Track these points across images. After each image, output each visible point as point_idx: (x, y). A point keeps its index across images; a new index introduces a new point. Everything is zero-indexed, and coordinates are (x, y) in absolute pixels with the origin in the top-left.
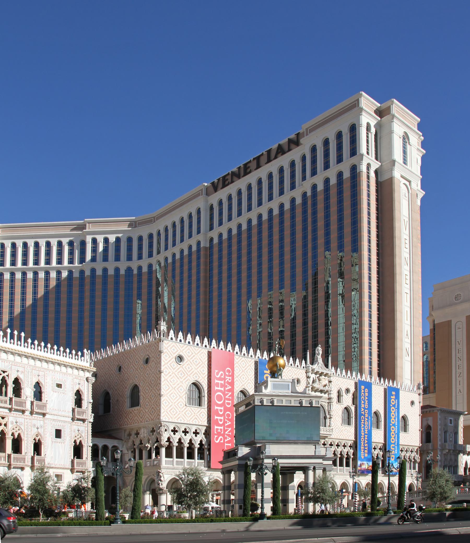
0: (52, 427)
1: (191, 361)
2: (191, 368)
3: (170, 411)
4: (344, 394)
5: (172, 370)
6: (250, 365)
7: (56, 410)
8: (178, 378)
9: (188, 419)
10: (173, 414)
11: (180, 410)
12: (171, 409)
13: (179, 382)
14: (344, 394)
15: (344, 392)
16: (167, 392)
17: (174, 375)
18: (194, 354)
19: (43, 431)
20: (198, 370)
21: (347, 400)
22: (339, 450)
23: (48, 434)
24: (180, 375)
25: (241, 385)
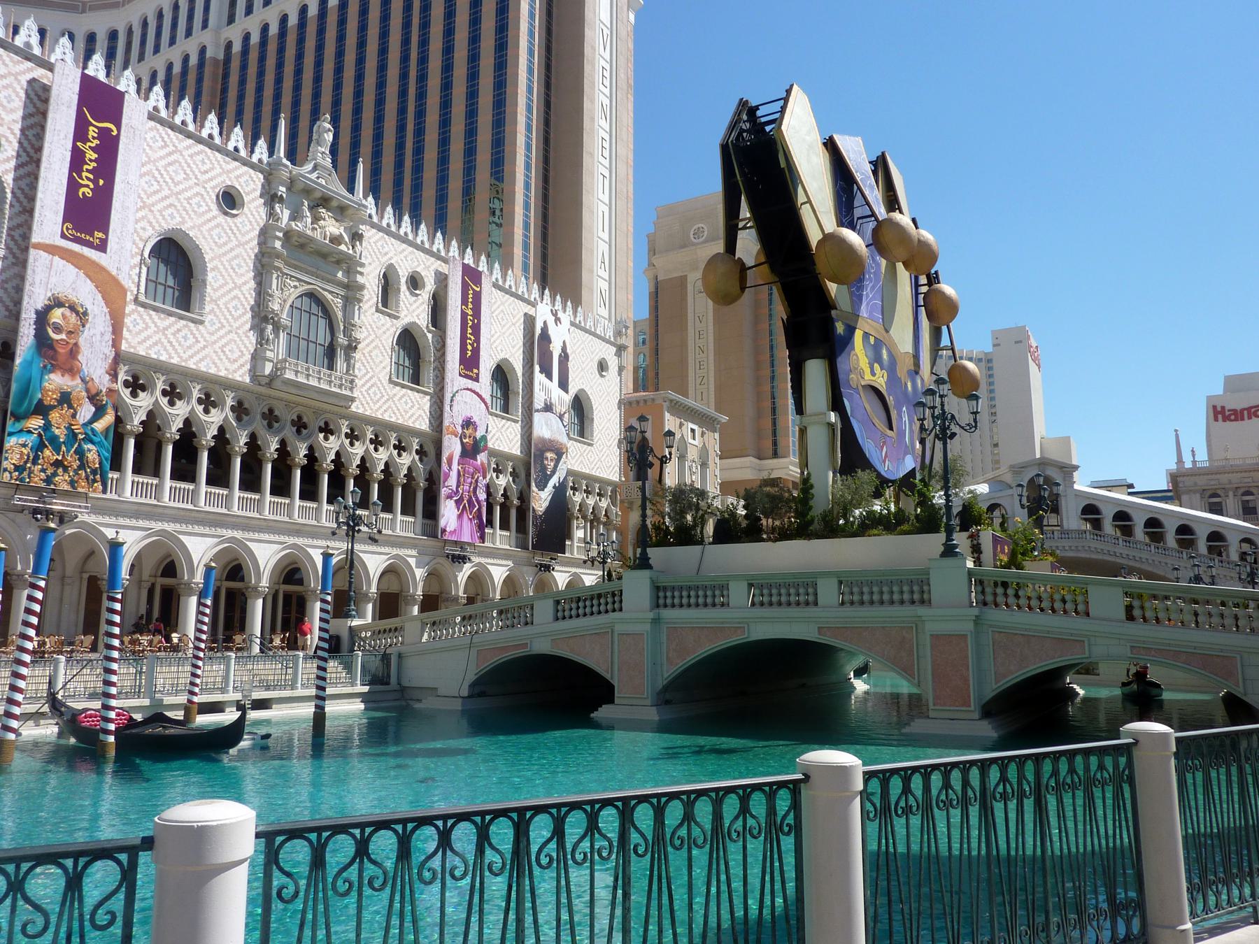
4: (403, 288)
6: (16, 75)
14: (403, 288)
15: (403, 280)
21: (415, 310)
22: (358, 450)
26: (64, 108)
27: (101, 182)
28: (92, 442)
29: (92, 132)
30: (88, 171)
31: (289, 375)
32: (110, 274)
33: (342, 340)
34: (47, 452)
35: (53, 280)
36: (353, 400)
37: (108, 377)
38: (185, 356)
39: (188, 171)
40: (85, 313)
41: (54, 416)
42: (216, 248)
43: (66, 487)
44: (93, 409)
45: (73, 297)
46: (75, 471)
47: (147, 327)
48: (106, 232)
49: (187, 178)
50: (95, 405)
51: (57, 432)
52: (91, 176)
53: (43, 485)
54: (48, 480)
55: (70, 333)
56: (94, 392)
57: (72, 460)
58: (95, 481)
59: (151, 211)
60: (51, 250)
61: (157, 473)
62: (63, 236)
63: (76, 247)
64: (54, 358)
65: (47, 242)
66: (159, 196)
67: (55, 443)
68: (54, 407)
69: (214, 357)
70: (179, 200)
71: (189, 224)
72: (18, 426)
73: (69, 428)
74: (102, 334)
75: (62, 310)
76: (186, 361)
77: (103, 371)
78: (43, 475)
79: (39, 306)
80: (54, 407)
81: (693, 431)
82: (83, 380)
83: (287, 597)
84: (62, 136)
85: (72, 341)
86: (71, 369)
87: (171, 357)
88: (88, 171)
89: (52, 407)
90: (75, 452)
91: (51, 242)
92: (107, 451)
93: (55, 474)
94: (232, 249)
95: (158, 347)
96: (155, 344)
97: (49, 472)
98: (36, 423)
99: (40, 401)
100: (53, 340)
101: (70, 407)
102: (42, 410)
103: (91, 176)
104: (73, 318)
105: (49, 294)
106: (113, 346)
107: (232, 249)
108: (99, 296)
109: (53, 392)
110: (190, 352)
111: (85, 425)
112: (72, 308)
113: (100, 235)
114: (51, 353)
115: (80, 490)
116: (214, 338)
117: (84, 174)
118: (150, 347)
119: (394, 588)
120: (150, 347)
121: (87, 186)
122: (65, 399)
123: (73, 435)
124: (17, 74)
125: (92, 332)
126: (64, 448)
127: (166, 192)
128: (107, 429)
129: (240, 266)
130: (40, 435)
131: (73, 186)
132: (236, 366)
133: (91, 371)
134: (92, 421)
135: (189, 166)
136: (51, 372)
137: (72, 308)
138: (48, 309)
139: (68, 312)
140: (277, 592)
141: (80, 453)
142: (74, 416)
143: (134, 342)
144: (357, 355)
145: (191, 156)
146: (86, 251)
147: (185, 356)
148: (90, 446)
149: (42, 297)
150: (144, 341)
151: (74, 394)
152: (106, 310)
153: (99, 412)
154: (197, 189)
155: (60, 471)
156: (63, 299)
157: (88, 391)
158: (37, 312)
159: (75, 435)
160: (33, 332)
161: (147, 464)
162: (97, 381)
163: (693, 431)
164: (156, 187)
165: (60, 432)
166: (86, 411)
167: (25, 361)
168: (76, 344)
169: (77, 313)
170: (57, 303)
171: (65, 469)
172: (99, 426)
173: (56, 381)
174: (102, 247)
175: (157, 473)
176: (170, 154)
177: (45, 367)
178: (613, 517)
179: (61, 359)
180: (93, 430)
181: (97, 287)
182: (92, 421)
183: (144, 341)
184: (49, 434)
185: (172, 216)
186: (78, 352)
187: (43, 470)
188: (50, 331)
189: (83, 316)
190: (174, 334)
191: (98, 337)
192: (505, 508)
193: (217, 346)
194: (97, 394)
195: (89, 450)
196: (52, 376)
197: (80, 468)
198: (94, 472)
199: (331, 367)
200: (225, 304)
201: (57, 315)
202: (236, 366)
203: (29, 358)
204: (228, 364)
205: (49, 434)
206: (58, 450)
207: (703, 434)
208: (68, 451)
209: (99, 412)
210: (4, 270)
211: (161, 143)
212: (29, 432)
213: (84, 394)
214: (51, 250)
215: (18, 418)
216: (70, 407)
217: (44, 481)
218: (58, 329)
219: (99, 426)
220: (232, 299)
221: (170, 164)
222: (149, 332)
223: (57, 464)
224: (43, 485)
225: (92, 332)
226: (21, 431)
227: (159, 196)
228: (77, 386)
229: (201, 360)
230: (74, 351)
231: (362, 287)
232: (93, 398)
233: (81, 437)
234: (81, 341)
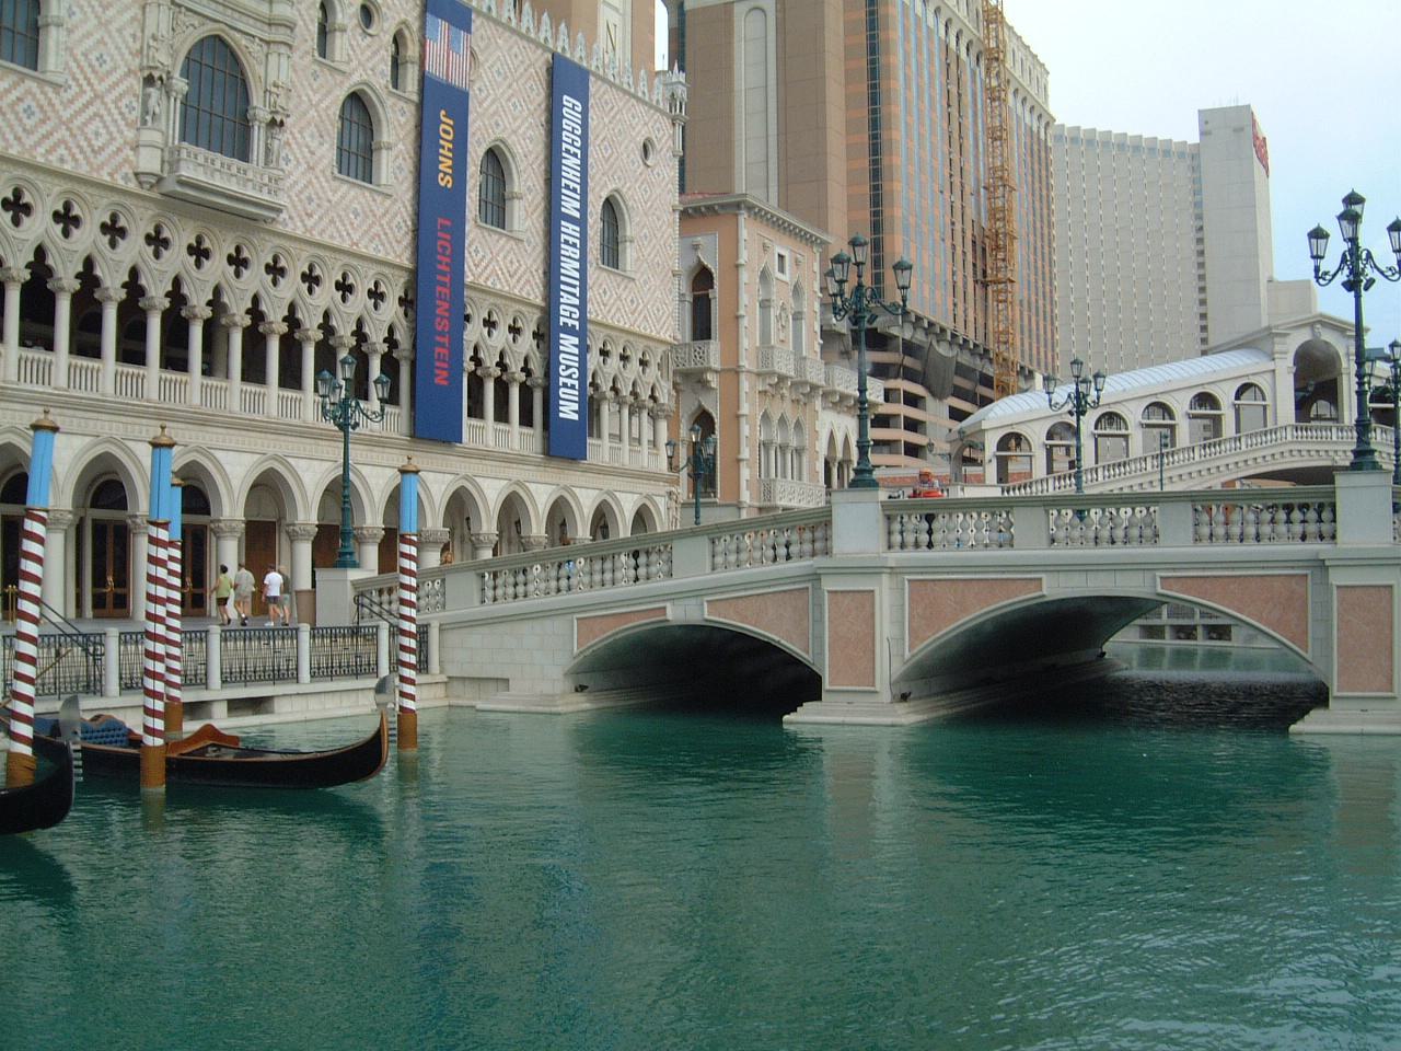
31: (188, 171)
33: (260, 110)
36: (279, 211)
61: (49, 346)
81: (781, 257)
83: (100, 529)
119: (268, 514)
140: (82, 520)
144: (285, 136)
163: (781, 257)
175: (49, 346)
178: (663, 398)
192: (502, 388)
199: (243, 154)
207: (797, 263)
210: (989, 53)
231: (290, 26)
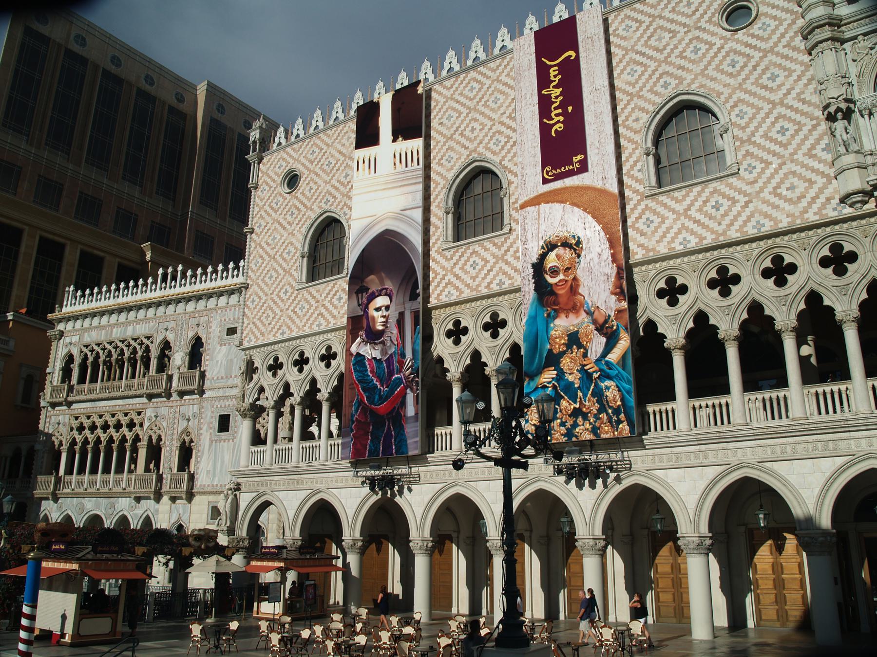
0: (212, 412)
1: (317, 170)
2: (315, 187)
3: (259, 319)
5: (273, 214)
7: (222, 378)
8: (284, 228)
9: (301, 324)
10: (267, 323)
11: (282, 305)
12: (264, 313)
13: (286, 235)
16: (258, 274)
17: (276, 225)
18: (325, 148)
19: (196, 423)
20: (334, 182)
23: (205, 427)
24: (289, 218)
25: (467, 153)
26: (526, 73)
27: (570, 109)
28: (609, 378)
29: (553, 72)
30: (555, 108)
32: (594, 189)
34: (564, 403)
35: (543, 227)
37: (614, 297)
38: (720, 229)
39: (673, 27)
40: (579, 243)
41: (566, 363)
42: (731, 81)
43: (588, 436)
44: (604, 340)
45: (563, 234)
46: (597, 417)
47: (664, 219)
48: (584, 151)
49: (674, 33)
50: (604, 335)
51: (570, 378)
52: (560, 111)
53: (564, 439)
54: (569, 434)
55: (568, 269)
56: (601, 320)
57: (591, 405)
58: (619, 422)
59: (640, 97)
60: (536, 201)
62: (545, 181)
63: (558, 184)
64: (556, 303)
65: (532, 196)
66: (647, 75)
67: (570, 391)
68: (564, 353)
69: (765, 208)
70: (670, 64)
71: (689, 77)
72: (533, 385)
73: (583, 370)
74: (600, 255)
75: (555, 251)
76: (724, 233)
77: (608, 293)
78: (563, 430)
79: (535, 260)
80: (564, 353)
82: (588, 313)
84: (528, 96)
85: (571, 277)
86: (574, 308)
87: (702, 238)
88: (555, 108)
89: (562, 354)
90: (593, 395)
91: (536, 194)
92: (628, 382)
93: (575, 425)
94: (755, 68)
95: (684, 234)
96: (679, 232)
97: (568, 425)
98: (549, 375)
99: (550, 351)
100: (551, 285)
101: (580, 346)
102: (553, 360)
103: (560, 111)
104: (567, 254)
105: (542, 243)
106: (614, 261)
107: (755, 68)
108: (589, 217)
109: (560, 337)
110: (727, 220)
111: (598, 361)
112: (565, 244)
113: (580, 157)
114: (552, 298)
115: (603, 436)
116: (760, 184)
117: (553, 115)
118: (673, 239)
120: (673, 239)
121: (559, 122)
122: (574, 340)
123: (586, 376)
124: (498, 77)
125: (588, 258)
126: (580, 394)
127: (653, 65)
128: (624, 357)
129: (773, 78)
130: (554, 387)
131: (545, 129)
132: (804, 203)
133: (595, 299)
134: (605, 354)
135: (672, 21)
136: (555, 318)
137: (565, 244)
138: (543, 257)
139: (560, 251)
141: (599, 394)
142: (585, 355)
143: (651, 244)
145: (673, 10)
146: (569, 182)
147: (720, 229)
148: (608, 383)
149: (536, 249)
150: (664, 236)
151: (581, 331)
152: (598, 228)
153: (612, 339)
154: (690, 35)
155: (580, 420)
156: (554, 239)
157: (594, 322)
158: (534, 266)
159: (589, 375)
160: (532, 286)
161: (707, 380)
162: (602, 307)
164: (640, 69)
165: (574, 378)
166: (597, 344)
167: (530, 317)
168: (575, 279)
169: (570, 246)
170: (551, 246)
171: (585, 417)
172: (614, 356)
173: (563, 324)
174: (584, 167)
176: (648, 27)
177: (549, 315)
179: (562, 300)
180: (608, 363)
181: (585, 210)
182: (605, 354)
183: (664, 236)
184: (563, 383)
185: (666, 85)
186: (578, 286)
187: (563, 424)
188: (548, 278)
189: (574, 246)
190: (700, 210)
191: (596, 260)
193: (766, 195)
194: (606, 322)
195: (608, 388)
196: (557, 322)
197: (600, 411)
198: (617, 411)
200: (765, 136)
201: (552, 260)
202: (804, 203)
203: (533, 314)
204: (787, 206)
205: (563, 383)
206: (574, 398)
208: (585, 395)
209: (612, 339)
211: (635, 25)
212: (544, 387)
213: (592, 327)
214: (536, 201)
215: (532, 377)
216: (580, 346)
217: (565, 435)
218: (554, 272)
219: (614, 356)
220: (773, 123)
221: (649, 38)
222: (668, 223)
223: (576, 413)
224: (564, 439)
225: (588, 258)
226: (537, 388)
227: (647, 75)
228: (583, 322)
229: (745, 223)
230: (574, 287)
232: (602, 328)
233: (595, 375)
234: (580, 273)
